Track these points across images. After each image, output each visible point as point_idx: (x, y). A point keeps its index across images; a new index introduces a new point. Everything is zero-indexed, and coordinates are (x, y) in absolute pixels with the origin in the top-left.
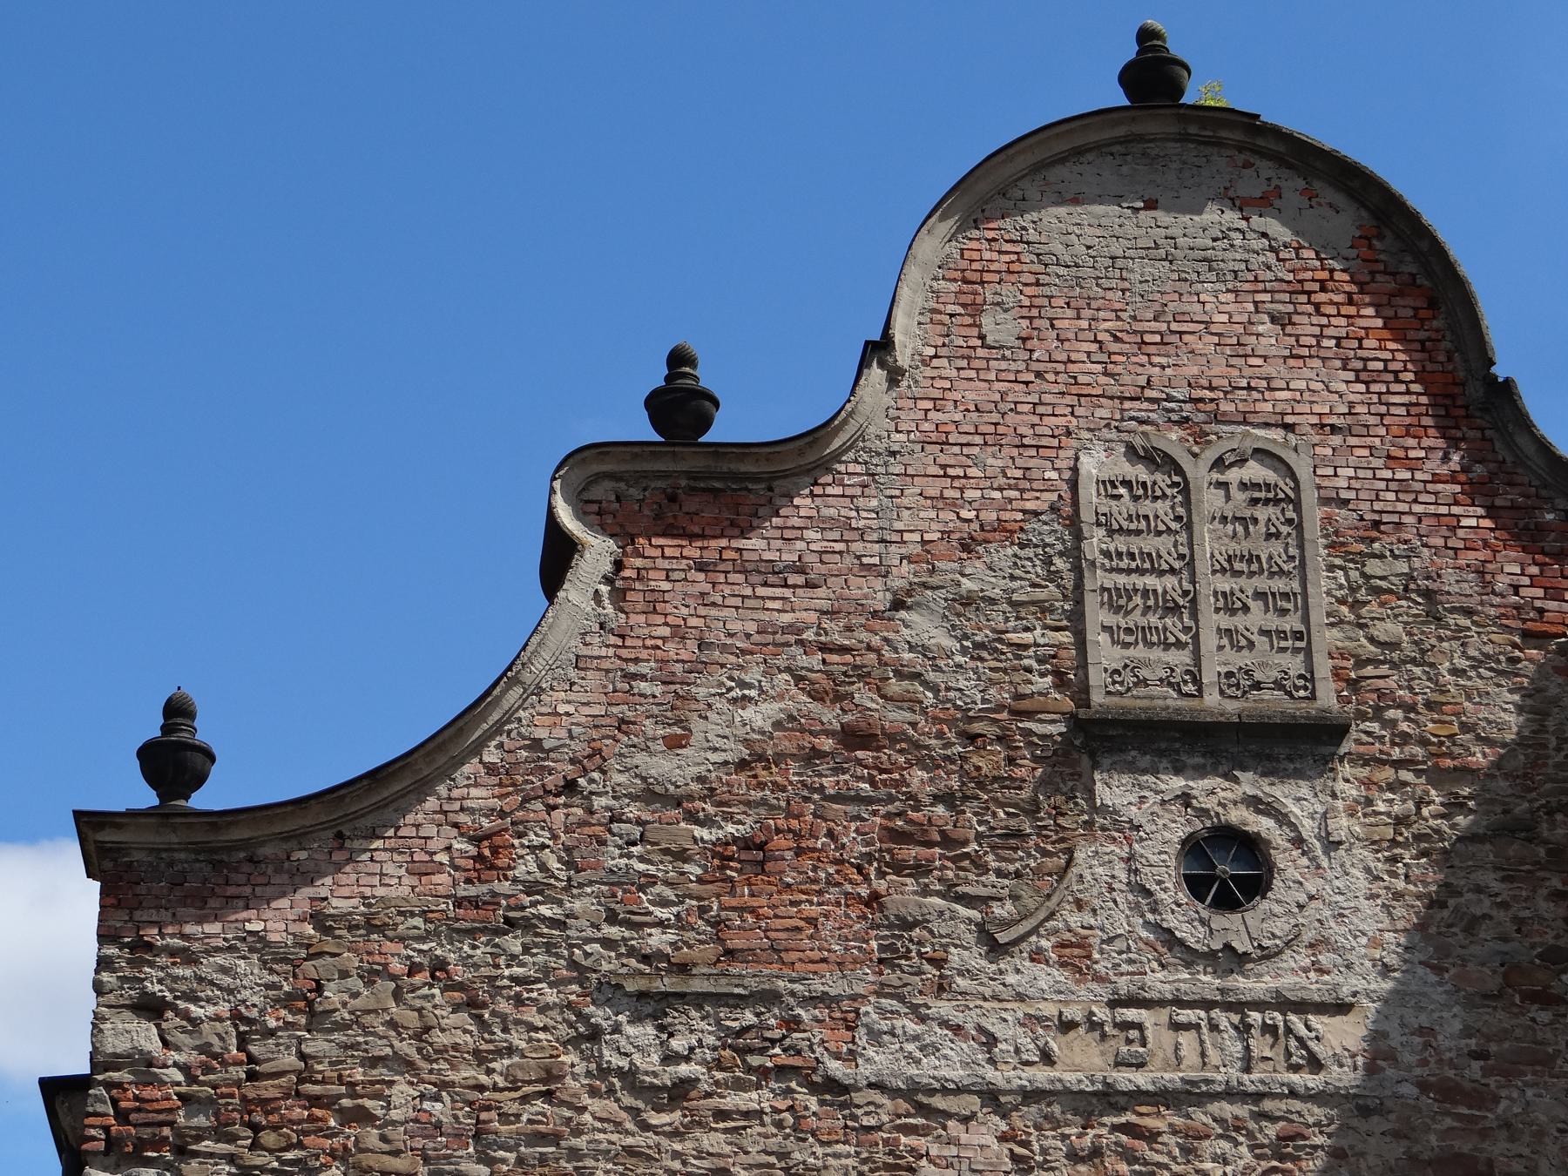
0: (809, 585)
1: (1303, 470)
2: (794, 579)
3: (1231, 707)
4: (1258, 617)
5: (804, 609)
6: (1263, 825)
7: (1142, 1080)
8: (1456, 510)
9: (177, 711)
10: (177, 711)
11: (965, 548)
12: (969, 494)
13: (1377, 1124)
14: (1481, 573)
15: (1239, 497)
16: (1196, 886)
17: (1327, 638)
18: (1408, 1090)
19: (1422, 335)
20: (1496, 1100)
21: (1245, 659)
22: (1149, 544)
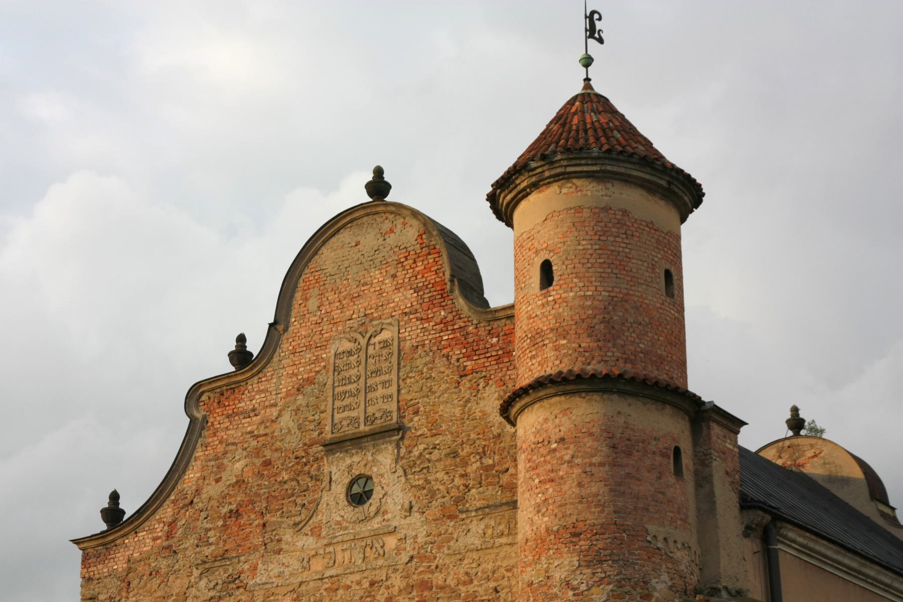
0: (256, 415)
3: (367, 428)
5: (250, 425)
8: (442, 334)
12: (301, 369)
14: (447, 357)
19: (436, 268)
20: (435, 558)
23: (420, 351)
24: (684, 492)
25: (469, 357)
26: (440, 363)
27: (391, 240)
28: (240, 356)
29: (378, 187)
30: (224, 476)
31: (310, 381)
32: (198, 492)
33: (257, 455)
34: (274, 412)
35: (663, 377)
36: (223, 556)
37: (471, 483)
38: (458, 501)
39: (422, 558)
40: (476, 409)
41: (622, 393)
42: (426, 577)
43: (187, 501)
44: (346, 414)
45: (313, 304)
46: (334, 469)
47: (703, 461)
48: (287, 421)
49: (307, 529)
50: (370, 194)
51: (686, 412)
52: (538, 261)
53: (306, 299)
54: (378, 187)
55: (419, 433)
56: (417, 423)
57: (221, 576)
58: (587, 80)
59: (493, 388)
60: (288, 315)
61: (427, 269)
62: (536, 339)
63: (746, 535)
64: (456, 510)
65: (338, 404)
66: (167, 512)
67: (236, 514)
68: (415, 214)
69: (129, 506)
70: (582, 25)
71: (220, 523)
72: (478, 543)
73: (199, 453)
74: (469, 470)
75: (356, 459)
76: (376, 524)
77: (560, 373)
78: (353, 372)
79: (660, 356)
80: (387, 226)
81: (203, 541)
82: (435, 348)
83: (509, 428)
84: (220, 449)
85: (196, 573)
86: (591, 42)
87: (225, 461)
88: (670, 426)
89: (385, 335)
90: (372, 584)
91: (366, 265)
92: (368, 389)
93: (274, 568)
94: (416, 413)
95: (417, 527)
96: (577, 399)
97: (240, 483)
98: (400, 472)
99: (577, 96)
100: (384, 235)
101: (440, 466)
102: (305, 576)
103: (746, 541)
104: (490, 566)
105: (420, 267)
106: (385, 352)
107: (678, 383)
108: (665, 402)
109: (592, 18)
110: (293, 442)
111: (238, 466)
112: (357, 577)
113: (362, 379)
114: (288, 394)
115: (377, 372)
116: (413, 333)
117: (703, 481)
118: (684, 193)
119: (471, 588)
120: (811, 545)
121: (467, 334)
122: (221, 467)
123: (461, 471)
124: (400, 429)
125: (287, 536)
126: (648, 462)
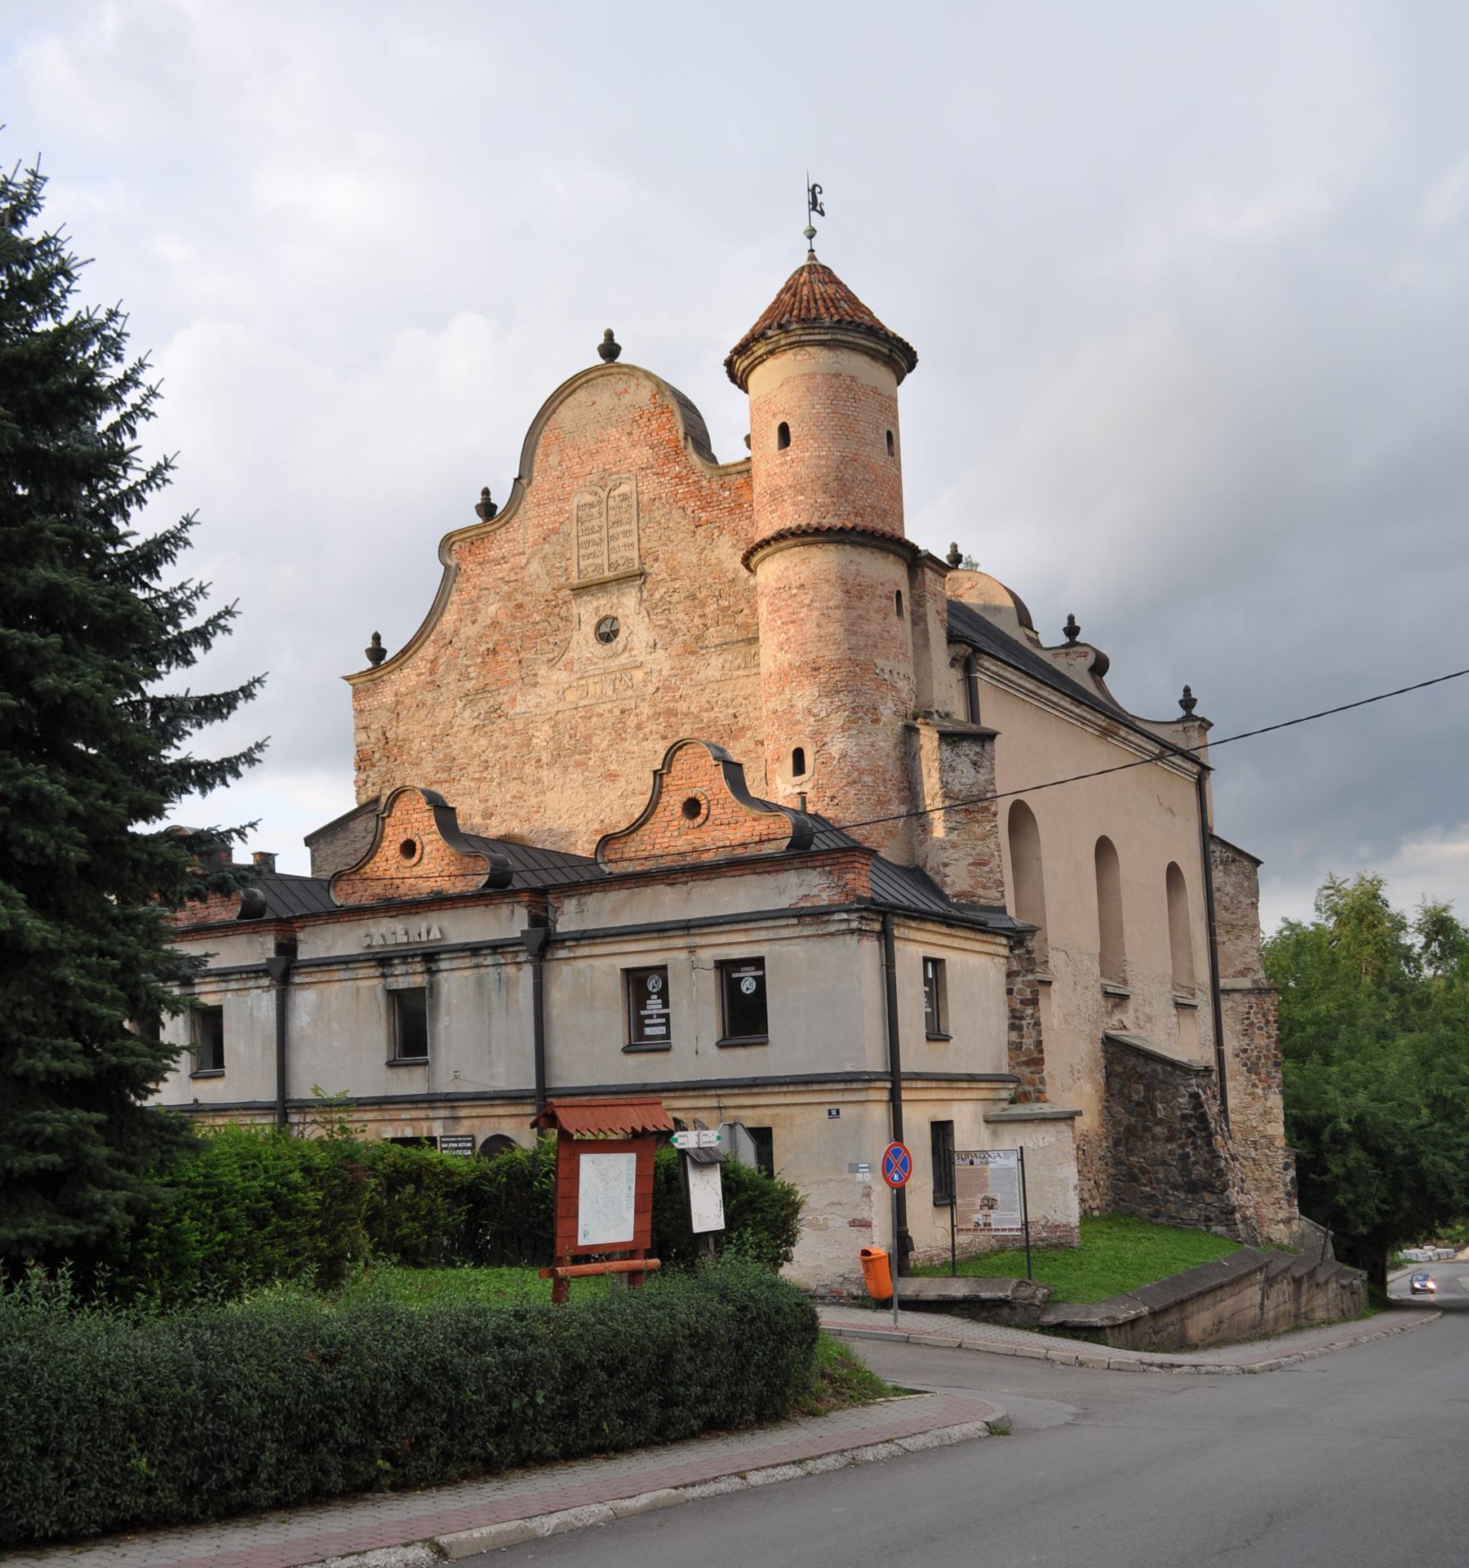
3: (611, 574)
5: (502, 571)
7: (586, 702)
23: (657, 503)
24: (903, 630)
25: (703, 509)
26: (677, 514)
27: (626, 399)
28: (487, 509)
29: (610, 350)
30: (480, 617)
31: (555, 531)
32: (456, 632)
33: (510, 599)
35: (887, 529)
36: (484, 690)
37: (709, 622)
38: (698, 638)
39: (667, 689)
40: (711, 556)
41: (853, 544)
42: (671, 705)
44: (591, 561)
45: (554, 459)
46: (582, 611)
47: (918, 602)
48: (535, 567)
49: (560, 665)
50: (603, 356)
51: (905, 559)
52: (776, 424)
53: (547, 455)
54: (610, 350)
56: (657, 569)
57: (483, 706)
58: (812, 251)
60: (531, 471)
61: (661, 427)
62: (776, 495)
63: (952, 665)
64: (696, 646)
65: (583, 552)
66: (428, 650)
67: (493, 652)
68: (648, 375)
69: (392, 648)
70: (806, 197)
71: (479, 660)
72: (717, 675)
73: (454, 597)
74: (707, 611)
75: (602, 602)
76: (623, 659)
77: (799, 526)
78: (596, 523)
79: (884, 510)
81: (464, 676)
83: (744, 573)
84: (474, 593)
85: (460, 704)
86: (814, 213)
88: (890, 572)
89: (624, 489)
90: (623, 712)
91: (603, 423)
92: (611, 538)
93: (532, 700)
94: (656, 560)
95: (661, 662)
96: (814, 550)
97: (495, 624)
98: (644, 613)
99: (803, 268)
100: (619, 395)
101: (680, 607)
102: (561, 706)
103: (952, 670)
104: (729, 695)
106: (624, 504)
107: (898, 533)
108: (889, 551)
109: (813, 191)
110: (543, 587)
111: (492, 608)
112: (609, 706)
113: (604, 530)
114: (535, 544)
115: (618, 523)
116: (650, 486)
117: (918, 619)
118: (900, 357)
119: (712, 715)
120: (1001, 672)
122: (476, 610)
124: (642, 574)
125: (543, 671)
126: (876, 604)
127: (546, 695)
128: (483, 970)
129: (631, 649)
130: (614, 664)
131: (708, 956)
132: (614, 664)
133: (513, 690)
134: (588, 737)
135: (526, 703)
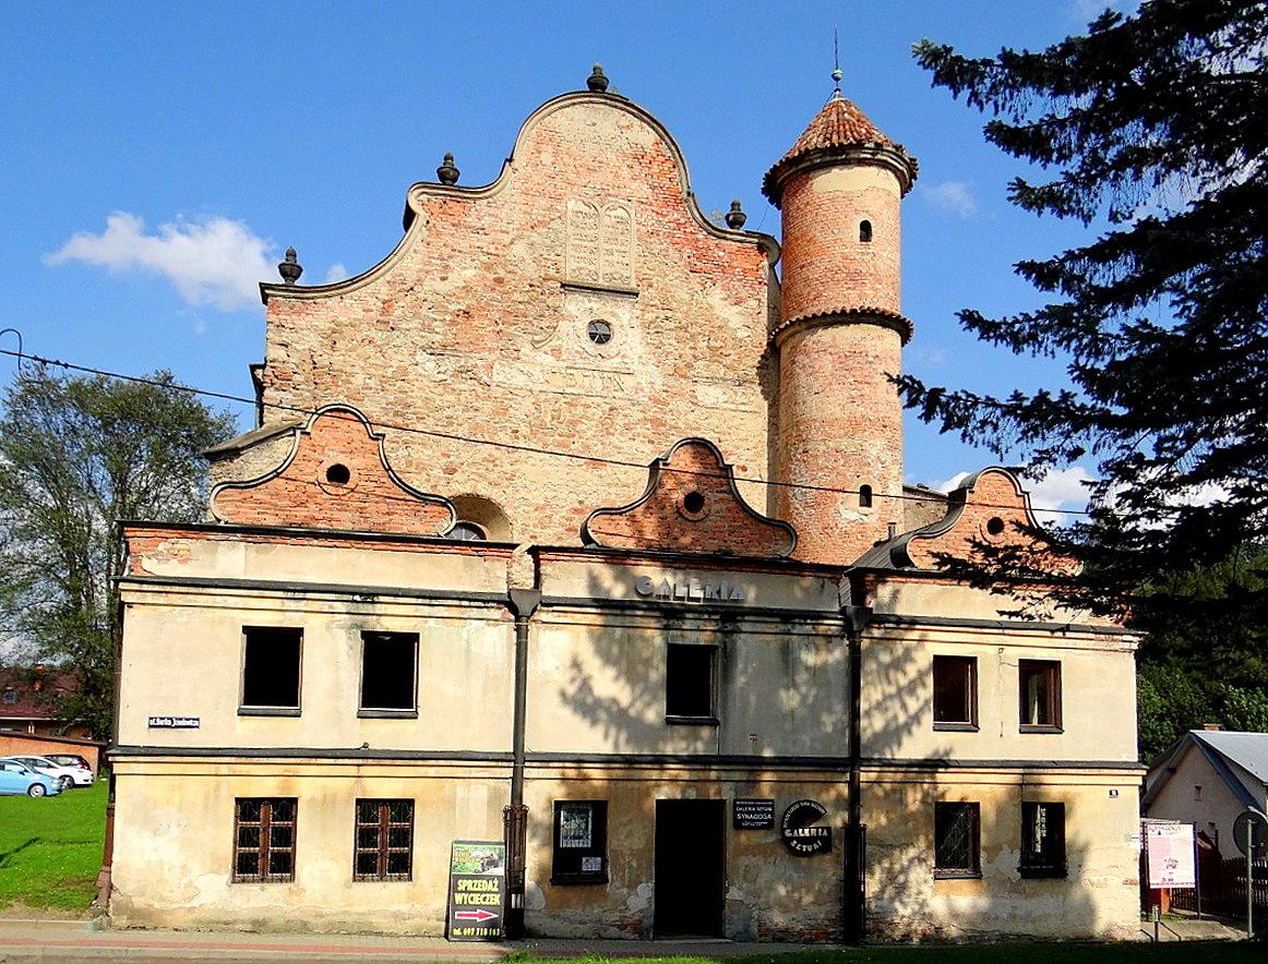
1: (633, 215)
2: (481, 232)
4: (616, 257)
5: (483, 241)
6: (611, 320)
9: (292, 254)
10: (292, 254)
11: (532, 228)
13: (636, 408)
15: (613, 219)
16: (592, 336)
17: (633, 266)
18: (646, 399)
21: (612, 270)
22: (588, 232)
34: (507, 240)
43: (407, 287)
48: (519, 249)
55: (652, 303)
57: (450, 364)
59: (718, 290)
61: (662, 173)
71: (448, 318)
75: (595, 306)
80: (624, 122)
82: (668, 240)
87: (450, 263)
89: (620, 212)
90: (611, 409)
94: (651, 286)
97: (467, 289)
105: (655, 169)
110: (532, 272)
111: (466, 272)
116: (649, 219)
121: (698, 240)
123: (692, 344)
125: (526, 349)
127: (528, 372)
128: (786, 637)
129: (624, 356)
130: (606, 365)
131: (1015, 655)
132: (606, 365)
133: (491, 357)
134: (573, 423)
135: (507, 375)
